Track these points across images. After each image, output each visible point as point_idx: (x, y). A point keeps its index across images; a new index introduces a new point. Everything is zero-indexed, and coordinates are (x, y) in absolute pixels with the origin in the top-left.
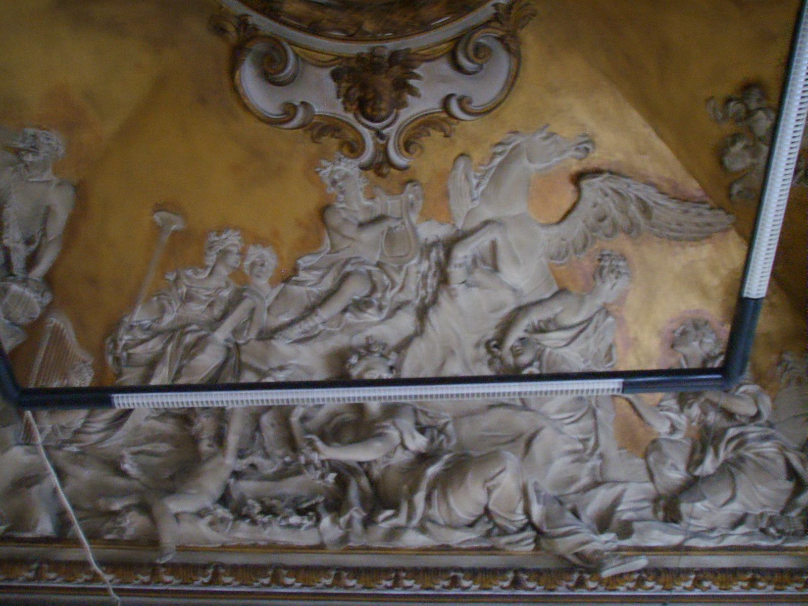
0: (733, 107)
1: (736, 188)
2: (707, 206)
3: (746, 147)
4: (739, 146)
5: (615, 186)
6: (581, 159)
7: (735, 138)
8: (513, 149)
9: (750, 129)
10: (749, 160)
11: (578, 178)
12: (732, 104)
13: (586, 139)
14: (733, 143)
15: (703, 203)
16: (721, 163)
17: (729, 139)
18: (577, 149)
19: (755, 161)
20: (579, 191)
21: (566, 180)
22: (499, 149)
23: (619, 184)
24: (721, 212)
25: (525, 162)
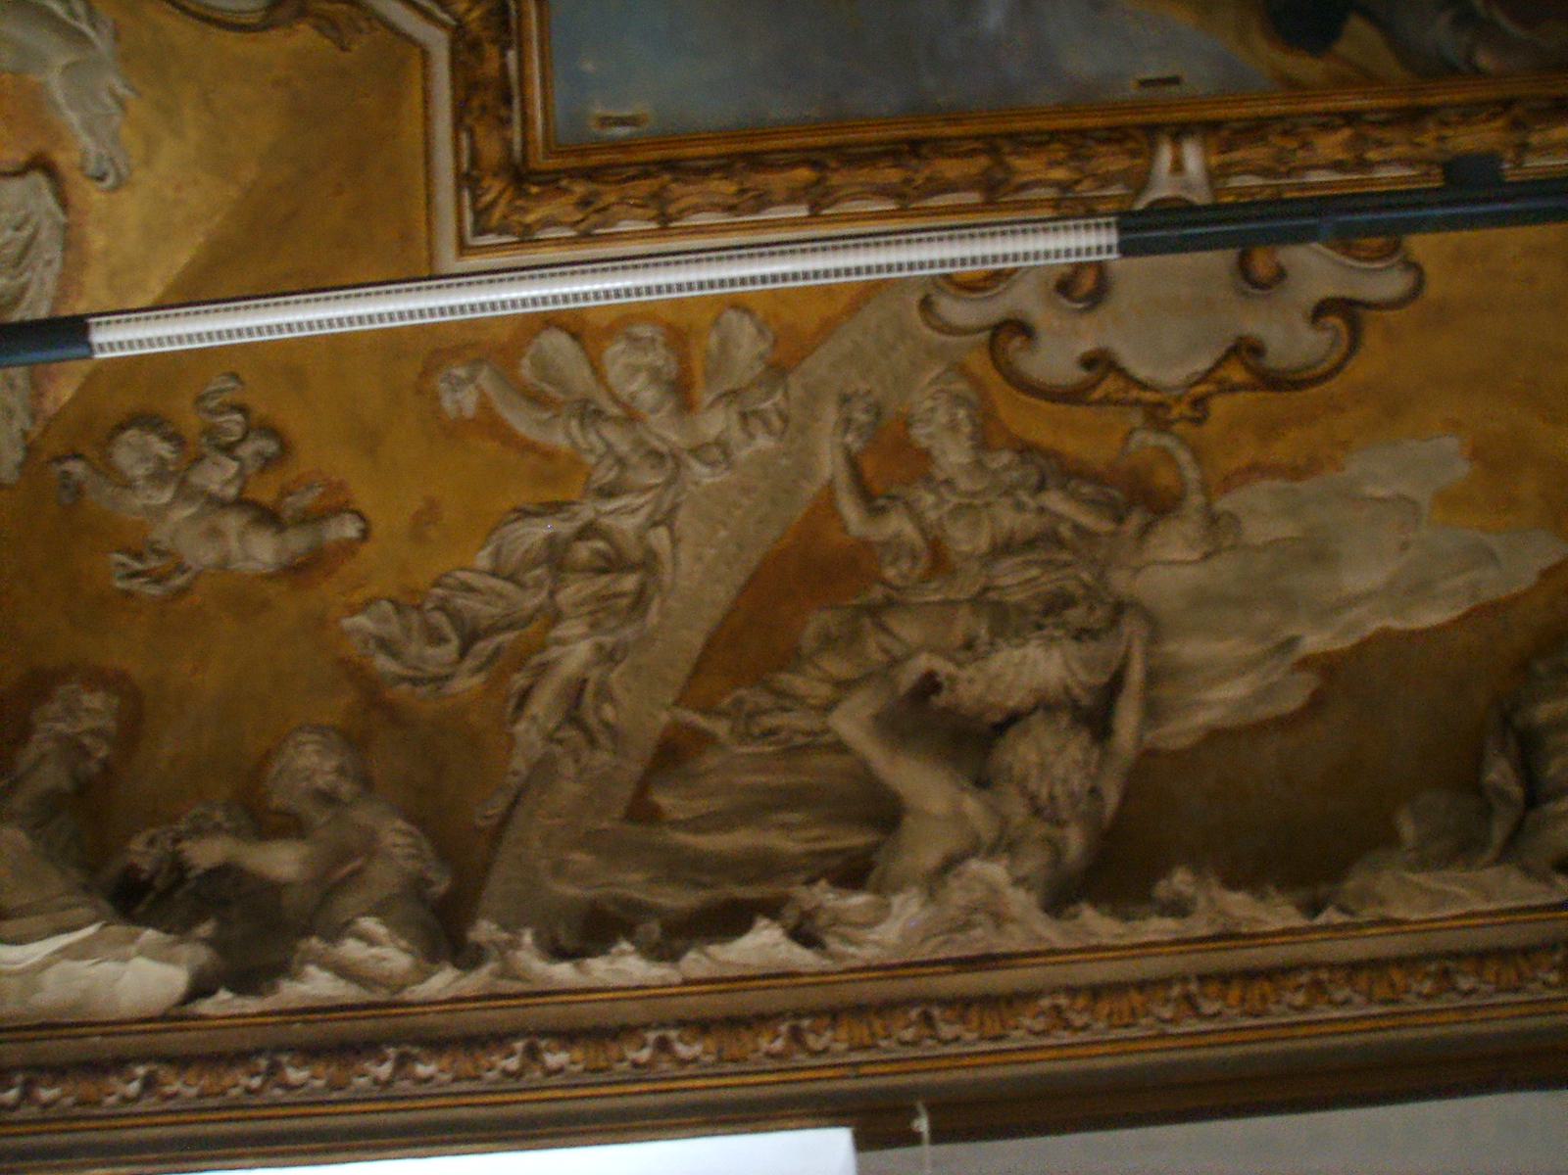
0: (233, 422)
1: (77, 468)
2: (28, 426)
3: (162, 461)
4: (164, 449)
5: (43, 236)
6: (82, 168)
7: (176, 439)
8: (81, 34)
9: (199, 459)
10: (140, 471)
11: (41, 164)
12: (238, 417)
13: (124, 171)
14: (167, 438)
15: (33, 417)
16: (122, 427)
17: (171, 429)
18: (100, 157)
19: (140, 483)
20: (20, 173)
21: (37, 144)
22: (80, 9)
23: (51, 250)
24: (18, 456)
25: (61, 61)
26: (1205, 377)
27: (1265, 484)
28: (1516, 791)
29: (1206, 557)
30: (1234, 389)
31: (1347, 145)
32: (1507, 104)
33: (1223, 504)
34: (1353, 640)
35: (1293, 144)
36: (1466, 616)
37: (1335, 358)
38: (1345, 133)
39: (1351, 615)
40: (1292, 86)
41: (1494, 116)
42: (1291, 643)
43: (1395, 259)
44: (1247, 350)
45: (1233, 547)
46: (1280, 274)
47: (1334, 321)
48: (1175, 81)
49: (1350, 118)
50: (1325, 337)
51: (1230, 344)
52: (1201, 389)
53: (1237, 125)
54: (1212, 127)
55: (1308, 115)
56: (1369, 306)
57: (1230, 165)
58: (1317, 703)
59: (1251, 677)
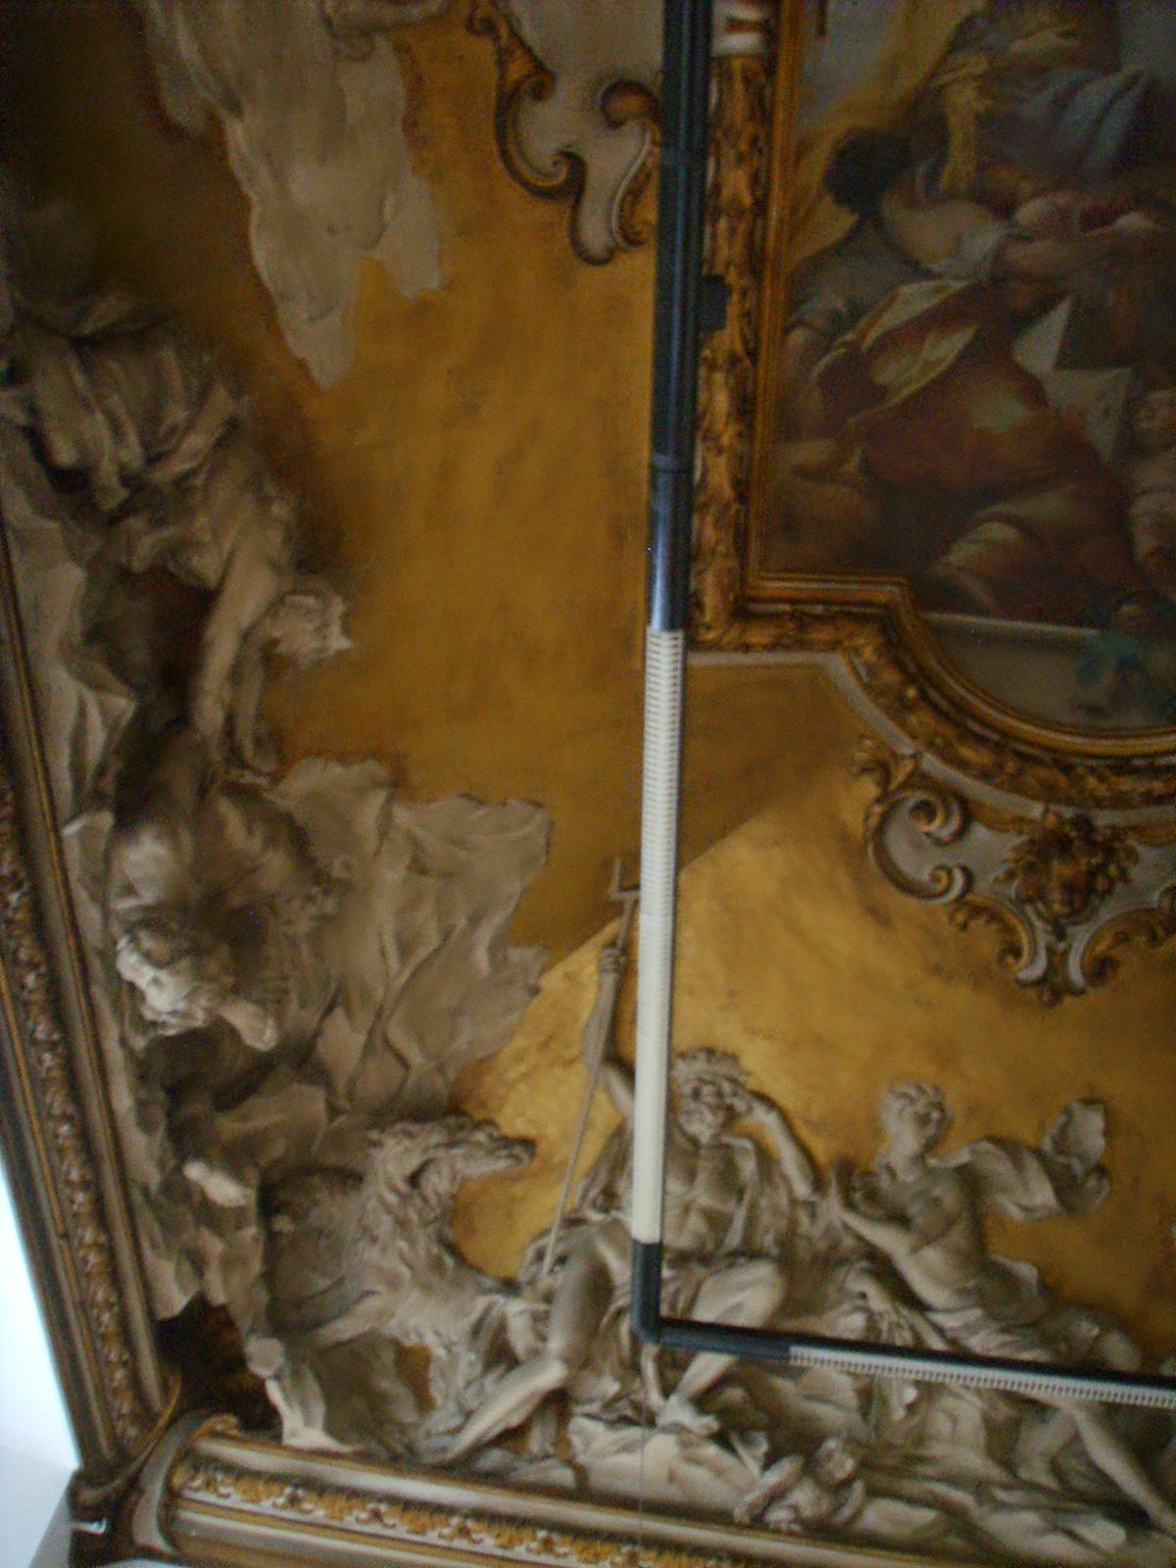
26: (516, 36)
27: (400, 89)
28: (88, 328)
29: (328, 22)
30: (501, 64)
31: (735, 200)
32: (753, 354)
33: (382, 45)
34: (240, 174)
35: (743, 146)
36: (259, 284)
37: (526, 172)
38: (747, 200)
39: (263, 172)
40: (802, 151)
41: (745, 341)
42: (236, 109)
43: (620, 240)
44: (541, 82)
45: (336, 53)
46: (615, 124)
47: (563, 175)
48: (822, 32)
49: (761, 206)
50: (547, 163)
51: (548, 65)
52: (504, 32)
53: (767, 93)
54: (770, 70)
55: (770, 162)
56: (577, 202)
57: (730, 79)
58: (172, 131)
59: (197, 58)
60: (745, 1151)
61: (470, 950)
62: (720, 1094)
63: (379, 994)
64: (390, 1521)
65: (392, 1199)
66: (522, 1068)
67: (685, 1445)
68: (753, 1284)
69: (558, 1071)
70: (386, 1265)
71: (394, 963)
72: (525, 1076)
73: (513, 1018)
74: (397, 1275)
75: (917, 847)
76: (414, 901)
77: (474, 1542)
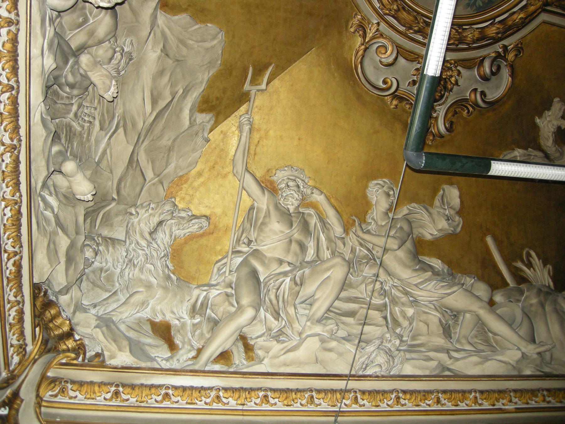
60: (310, 215)
61: (181, 110)
62: (298, 187)
63: (140, 125)
64: (174, 399)
65: (143, 243)
66: (201, 180)
67: (323, 341)
68: (333, 266)
69: (220, 180)
70: (143, 277)
71: (148, 108)
72: (203, 184)
73: (197, 154)
74: (150, 282)
75: (376, 68)
76: (161, 73)
77: (225, 404)
